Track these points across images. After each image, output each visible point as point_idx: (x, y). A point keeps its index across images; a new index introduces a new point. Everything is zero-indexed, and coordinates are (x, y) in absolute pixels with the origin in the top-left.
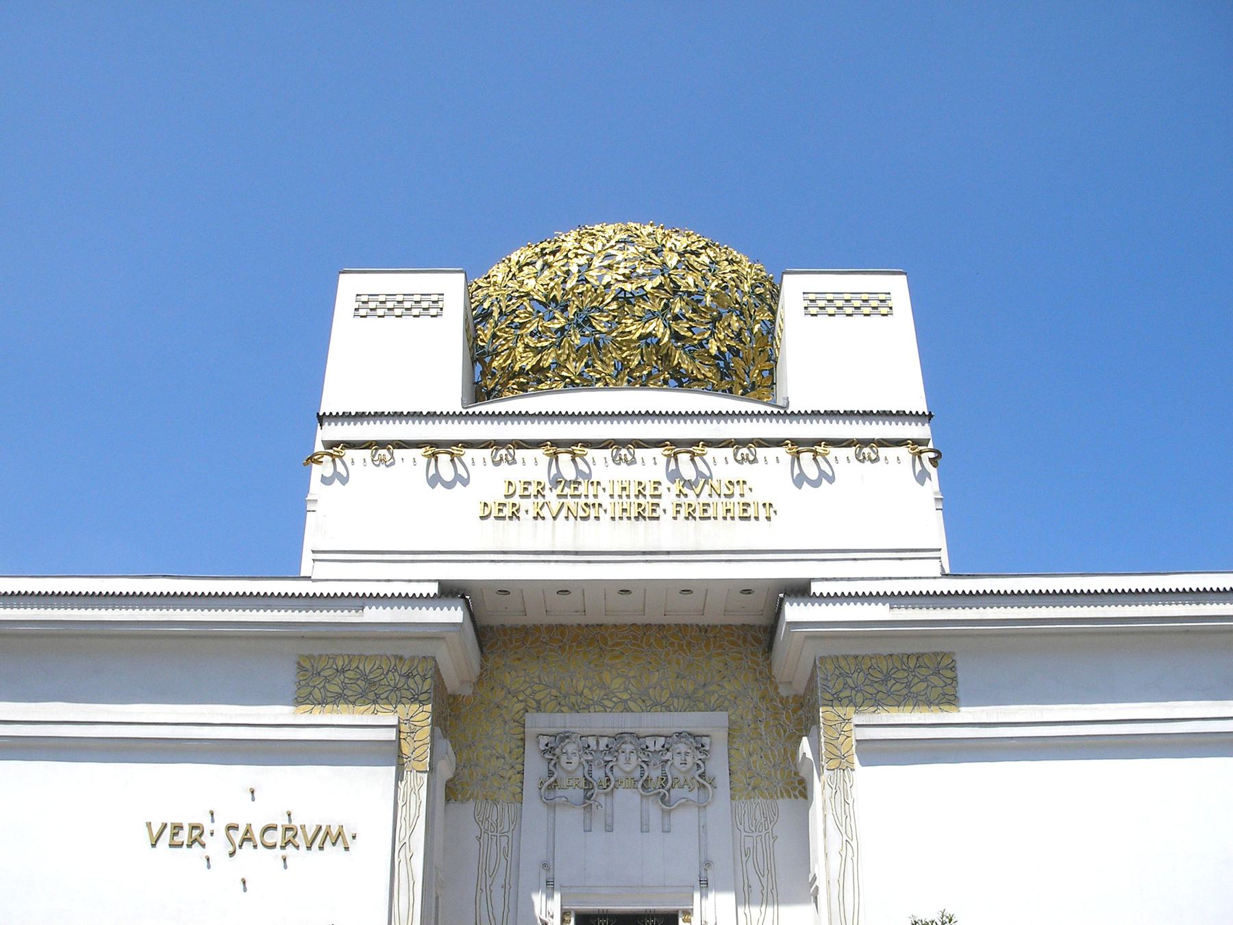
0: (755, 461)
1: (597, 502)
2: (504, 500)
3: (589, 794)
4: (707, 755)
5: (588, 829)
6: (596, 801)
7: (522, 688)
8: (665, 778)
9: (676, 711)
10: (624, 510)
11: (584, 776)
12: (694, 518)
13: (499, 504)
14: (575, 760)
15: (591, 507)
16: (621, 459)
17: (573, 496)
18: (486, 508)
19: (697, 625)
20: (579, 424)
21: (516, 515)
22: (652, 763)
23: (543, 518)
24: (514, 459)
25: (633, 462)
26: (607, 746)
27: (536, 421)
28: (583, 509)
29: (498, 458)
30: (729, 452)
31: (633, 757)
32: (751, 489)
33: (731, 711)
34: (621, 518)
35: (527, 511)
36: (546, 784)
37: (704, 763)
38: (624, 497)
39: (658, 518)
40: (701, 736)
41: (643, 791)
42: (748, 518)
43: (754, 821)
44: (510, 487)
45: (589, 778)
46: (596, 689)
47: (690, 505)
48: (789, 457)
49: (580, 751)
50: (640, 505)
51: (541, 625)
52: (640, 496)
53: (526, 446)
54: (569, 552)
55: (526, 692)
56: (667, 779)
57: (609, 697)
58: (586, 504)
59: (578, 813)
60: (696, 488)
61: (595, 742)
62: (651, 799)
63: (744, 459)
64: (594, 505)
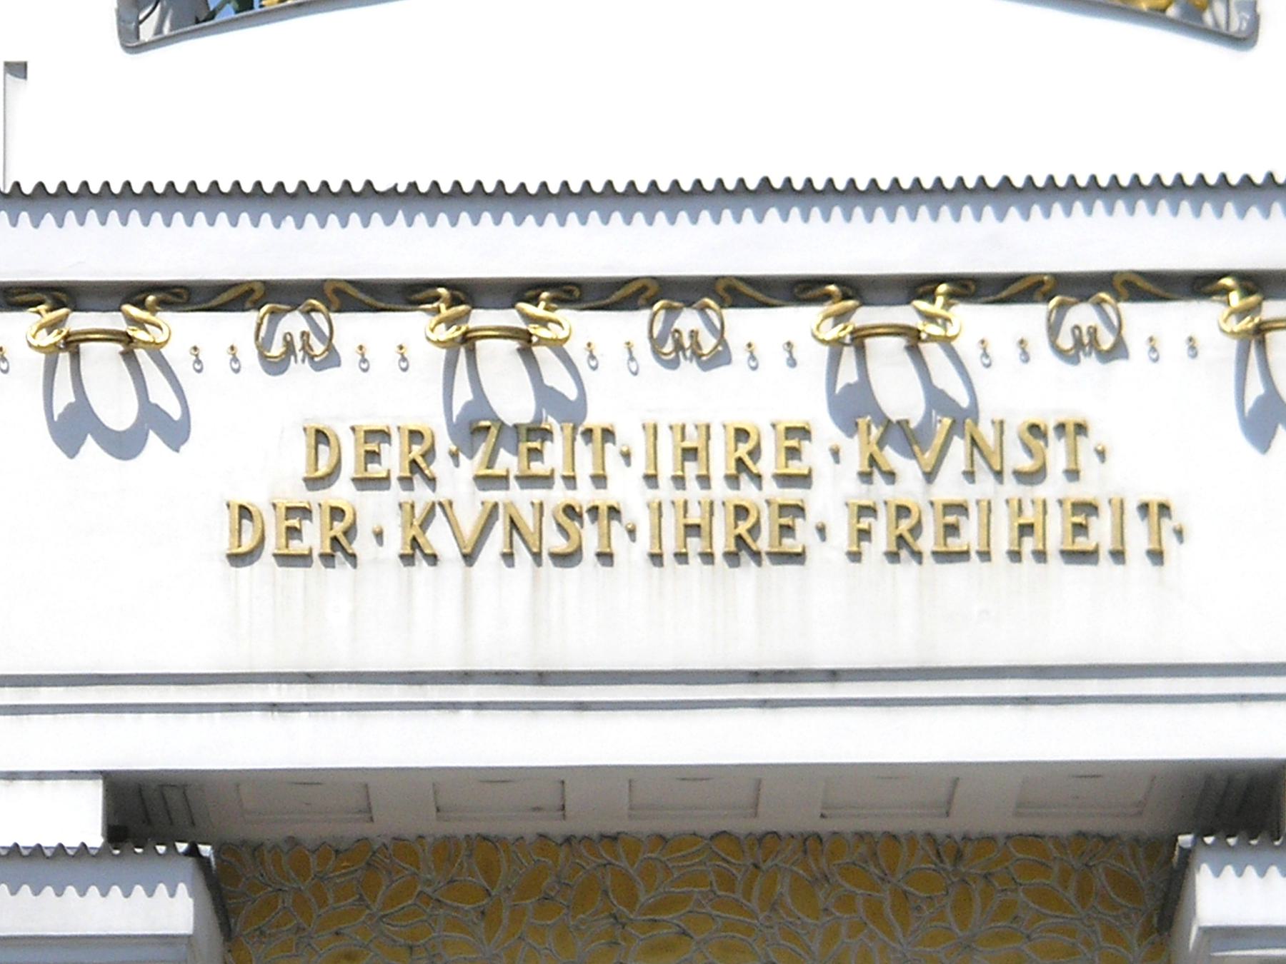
0: (1118, 350)
1: (602, 498)
2: (302, 496)
10: (692, 530)
12: (917, 555)
13: (291, 511)
15: (586, 516)
16: (679, 347)
17: (528, 480)
18: (245, 522)
20: (540, 223)
21: (344, 550)
23: (433, 559)
24: (330, 348)
25: (720, 357)
27: (400, 215)
28: (559, 525)
29: (277, 349)
30: (1031, 317)
32: (1101, 454)
34: (682, 557)
35: (379, 535)
38: (692, 484)
39: (797, 558)
42: (1087, 556)
44: (322, 447)
47: (903, 511)
48: (1232, 346)
50: (741, 512)
52: (744, 478)
53: (368, 299)
54: (517, 673)
58: (570, 511)
60: (923, 451)
63: (1085, 344)
64: (594, 510)
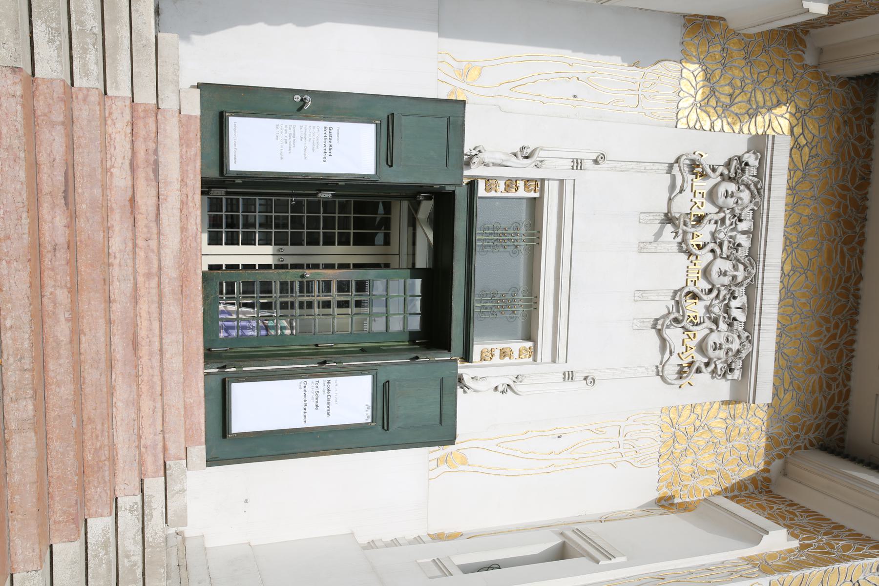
7: (806, 132)
8: (696, 322)
19: (853, 357)
26: (739, 245)
31: (726, 280)
40: (745, 369)
43: (636, 438)
46: (797, 231)
51: (872, 160)
55: (802, 136)
56: (697, 325)
57: (787, 248)
61: (746, 229)
62: (673, 302)
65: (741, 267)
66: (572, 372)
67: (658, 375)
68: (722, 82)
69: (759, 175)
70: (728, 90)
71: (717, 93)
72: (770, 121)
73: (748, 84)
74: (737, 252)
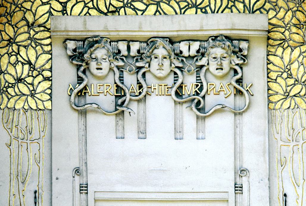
3: (120, 101)
4: (244, 61)
5: (120, 135)
6: (128, 108)
9: (213, 12)
11: (115, 83)
14: (105, 65)
22: (186, 70)
31: (167, 62)
33: (272, 14)
36: (76, 91)
37: (241, 68)
41: (178, 98)
45: (121, 85)
49: (109, 57)
59: (111, 120)
62: (185, 105)
65: (156, 51)
66: (235, 187)
67: (242, 114)
68: (14, 73)
69: (84, 40)
70: (19, 67)
71: (22, 77)
72: (39, 26)
73: (12, 49)
74: (144, 53)
